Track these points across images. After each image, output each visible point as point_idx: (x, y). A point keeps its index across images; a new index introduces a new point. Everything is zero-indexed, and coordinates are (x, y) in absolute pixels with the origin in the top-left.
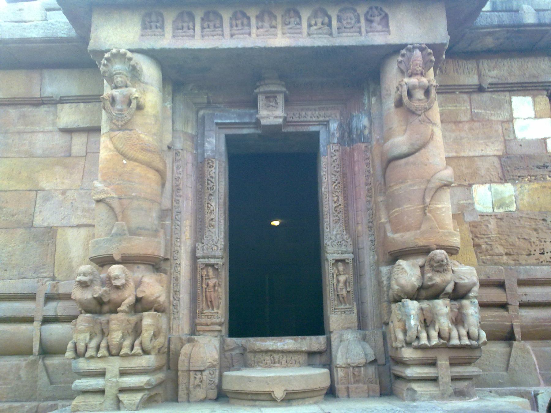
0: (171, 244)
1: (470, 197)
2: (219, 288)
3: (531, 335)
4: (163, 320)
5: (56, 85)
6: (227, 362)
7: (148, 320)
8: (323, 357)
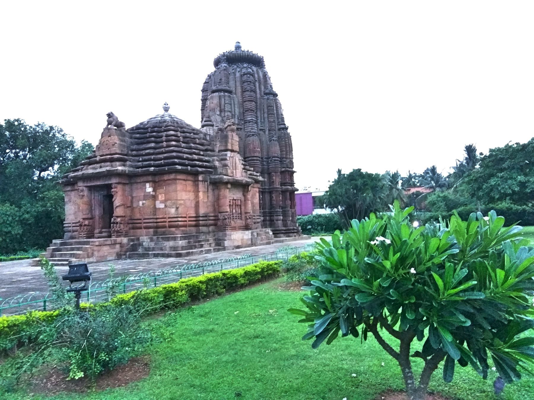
1: (139, 204)
4: (89, 227)
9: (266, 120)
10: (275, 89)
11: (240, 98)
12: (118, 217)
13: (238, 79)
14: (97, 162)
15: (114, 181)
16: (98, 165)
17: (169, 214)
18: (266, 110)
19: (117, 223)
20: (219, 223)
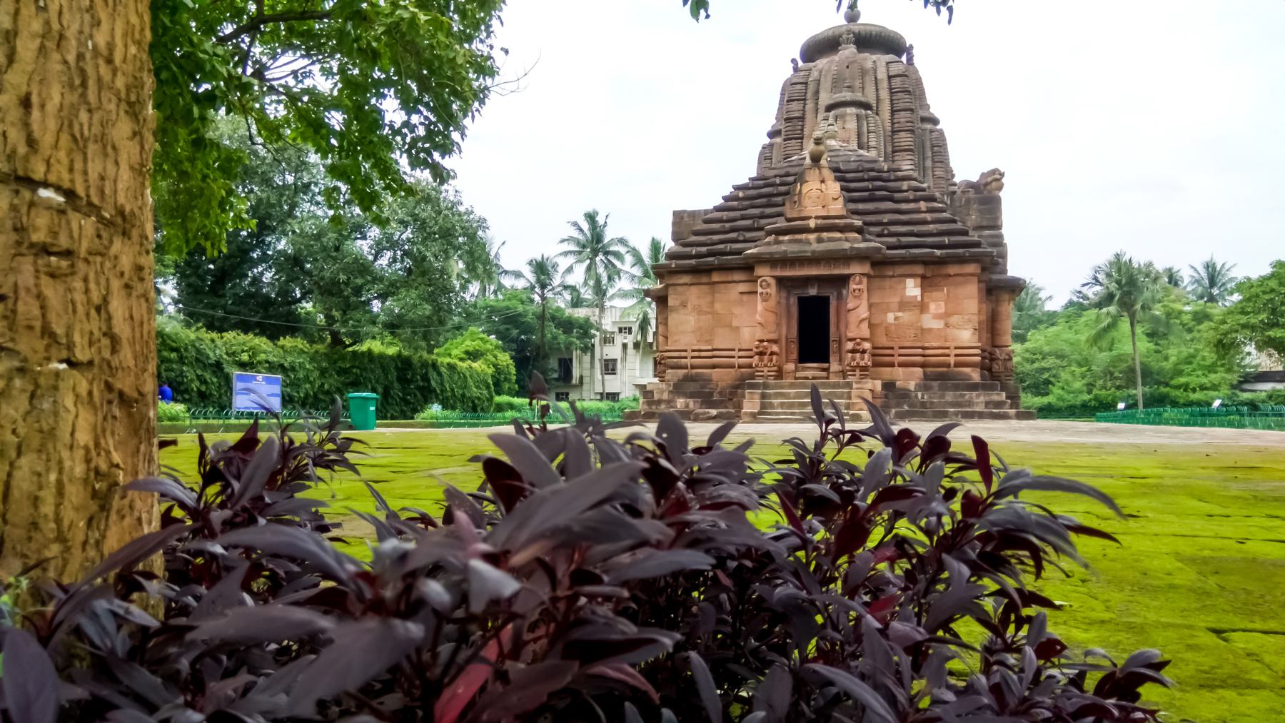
0: (780, 335)
2: (794, 348)
3: (901, 365)
5: (737, 276)
6: (797, 370)
7: (775, 357)
8: (827, 370)
9: (930, 172)
10: (935, 110)
11: (888, 124)
12: (863, 339)
13: (884, 85)
14: (807, 230)
15: (855, 269)
16: (812, 237)
17: (953, 340)
18: (929, 154)
19: (864, 352)
20: (996, 367)
